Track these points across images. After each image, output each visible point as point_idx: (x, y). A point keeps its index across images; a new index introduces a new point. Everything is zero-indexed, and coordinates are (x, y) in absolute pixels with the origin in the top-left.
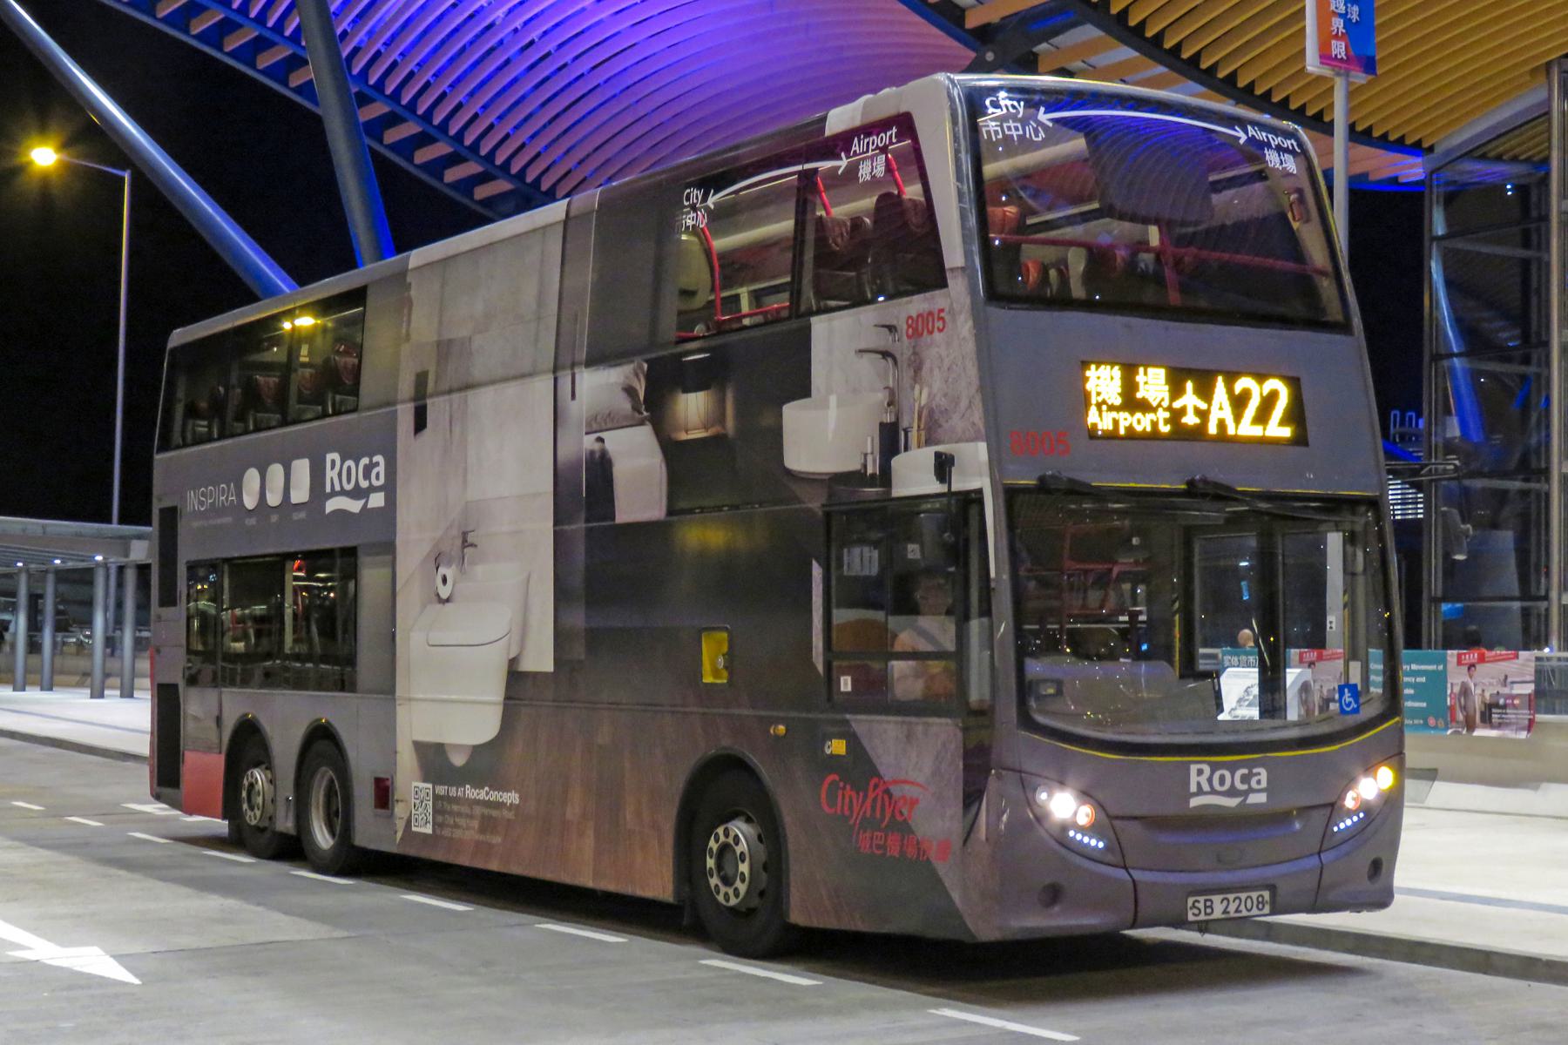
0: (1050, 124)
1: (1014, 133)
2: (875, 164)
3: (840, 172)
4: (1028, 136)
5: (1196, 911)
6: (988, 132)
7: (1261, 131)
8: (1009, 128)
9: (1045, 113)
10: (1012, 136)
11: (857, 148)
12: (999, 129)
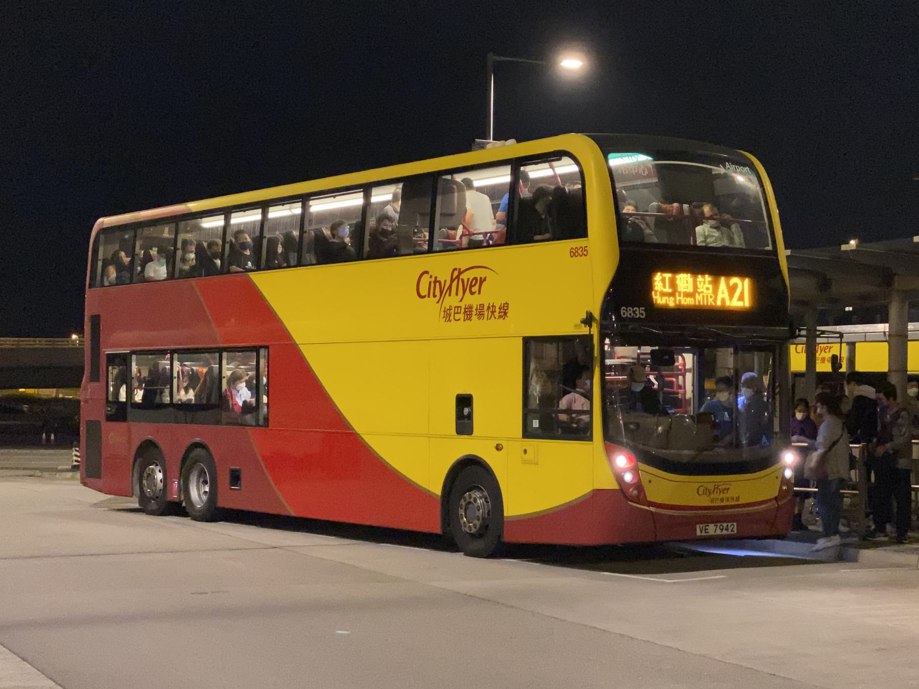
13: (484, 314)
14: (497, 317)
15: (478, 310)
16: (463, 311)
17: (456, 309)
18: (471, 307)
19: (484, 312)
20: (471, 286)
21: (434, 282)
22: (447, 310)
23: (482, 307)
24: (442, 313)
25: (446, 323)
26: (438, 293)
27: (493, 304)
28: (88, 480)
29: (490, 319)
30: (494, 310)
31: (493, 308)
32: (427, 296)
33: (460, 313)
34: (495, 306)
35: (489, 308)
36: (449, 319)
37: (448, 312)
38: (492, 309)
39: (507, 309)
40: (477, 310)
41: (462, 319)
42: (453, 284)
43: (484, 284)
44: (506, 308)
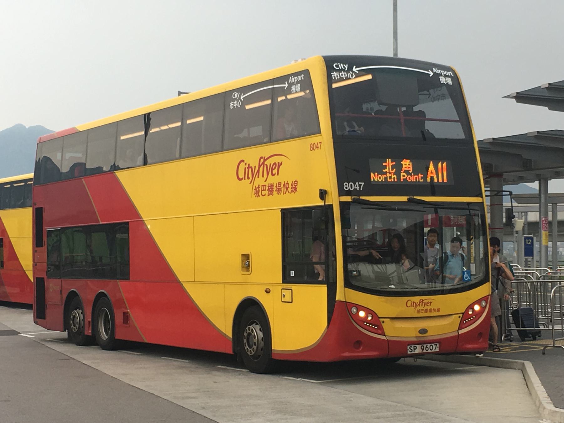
0: (357, 72)
1: (344, 76)
2: (297, 87)
3: (285, 89)
4: (349, 77)
5: (411, 351)
6: (334, 76)
7: (438, 69)
8: (342, 75)
9: (356, 68)
10: (343, 77)
11: (291, 81)
12: (338, 75)
13: (281, 190)
14: (290, 191)
15: (278, 187)
16: (267, 188)
17: (263, 187)
18: (272, 185)
19: (281, 188)
20: (273, 170)
21: (248, 168)
22: (257, 188)
23: (280, 185)
24: (254, 190)
25: (256, 197)
26: (250, 176)
27: (287, 182)
28: (38, 320)
29: (285, 193)
30: (288, 187)
31: (287, 185)
32: (243, 178)
33: (265, 190)
34: (288, 184)
35: (284, 185)
36: (258, 196)
37: (258, 190)
38: (286, 185)
39: (297, 185)
40: (276, 187)
41: (267, 195)
42: (260, 169)
43: (281, 166)
44: (295, 185)
